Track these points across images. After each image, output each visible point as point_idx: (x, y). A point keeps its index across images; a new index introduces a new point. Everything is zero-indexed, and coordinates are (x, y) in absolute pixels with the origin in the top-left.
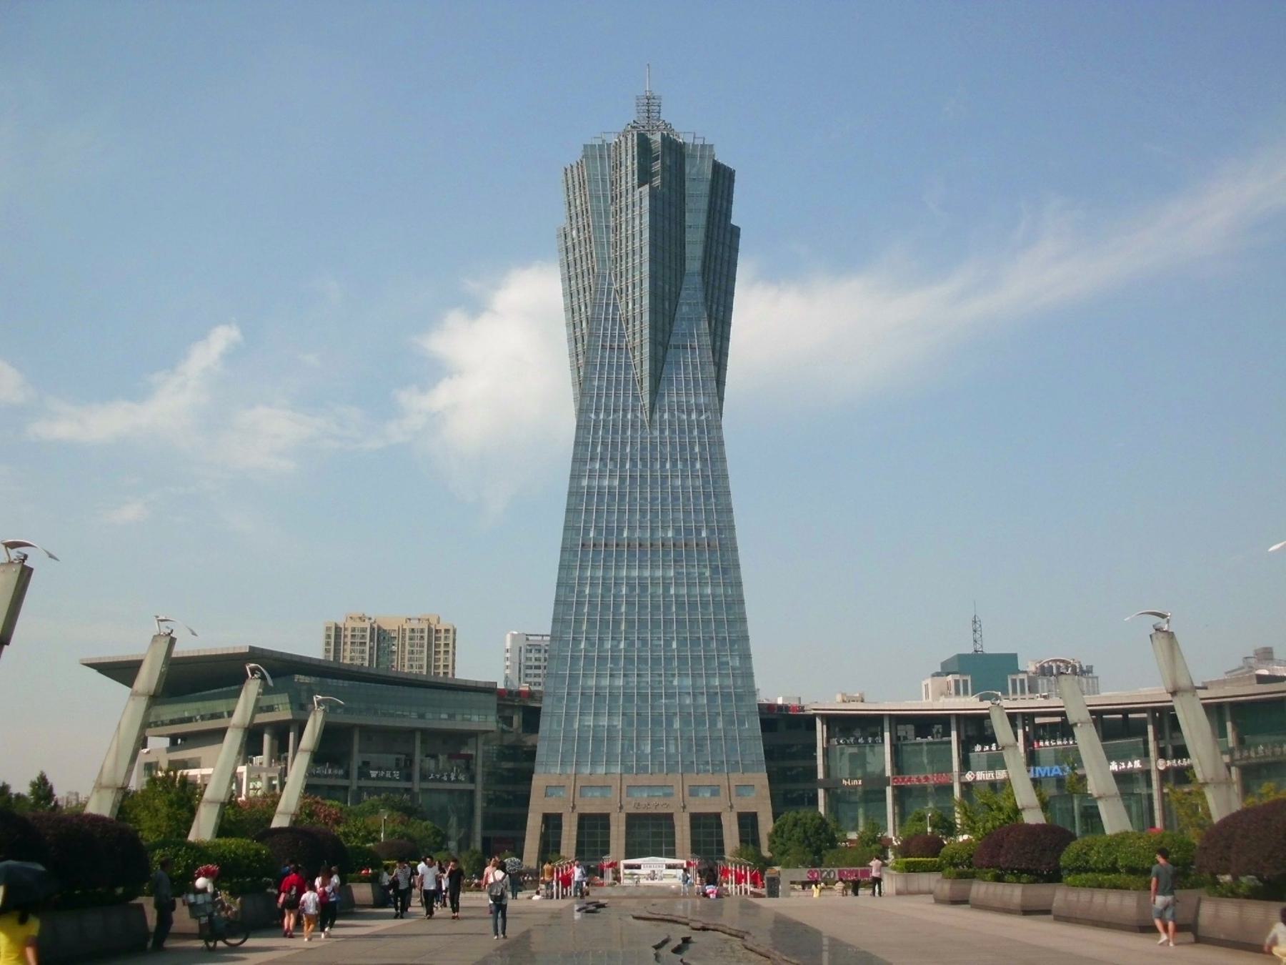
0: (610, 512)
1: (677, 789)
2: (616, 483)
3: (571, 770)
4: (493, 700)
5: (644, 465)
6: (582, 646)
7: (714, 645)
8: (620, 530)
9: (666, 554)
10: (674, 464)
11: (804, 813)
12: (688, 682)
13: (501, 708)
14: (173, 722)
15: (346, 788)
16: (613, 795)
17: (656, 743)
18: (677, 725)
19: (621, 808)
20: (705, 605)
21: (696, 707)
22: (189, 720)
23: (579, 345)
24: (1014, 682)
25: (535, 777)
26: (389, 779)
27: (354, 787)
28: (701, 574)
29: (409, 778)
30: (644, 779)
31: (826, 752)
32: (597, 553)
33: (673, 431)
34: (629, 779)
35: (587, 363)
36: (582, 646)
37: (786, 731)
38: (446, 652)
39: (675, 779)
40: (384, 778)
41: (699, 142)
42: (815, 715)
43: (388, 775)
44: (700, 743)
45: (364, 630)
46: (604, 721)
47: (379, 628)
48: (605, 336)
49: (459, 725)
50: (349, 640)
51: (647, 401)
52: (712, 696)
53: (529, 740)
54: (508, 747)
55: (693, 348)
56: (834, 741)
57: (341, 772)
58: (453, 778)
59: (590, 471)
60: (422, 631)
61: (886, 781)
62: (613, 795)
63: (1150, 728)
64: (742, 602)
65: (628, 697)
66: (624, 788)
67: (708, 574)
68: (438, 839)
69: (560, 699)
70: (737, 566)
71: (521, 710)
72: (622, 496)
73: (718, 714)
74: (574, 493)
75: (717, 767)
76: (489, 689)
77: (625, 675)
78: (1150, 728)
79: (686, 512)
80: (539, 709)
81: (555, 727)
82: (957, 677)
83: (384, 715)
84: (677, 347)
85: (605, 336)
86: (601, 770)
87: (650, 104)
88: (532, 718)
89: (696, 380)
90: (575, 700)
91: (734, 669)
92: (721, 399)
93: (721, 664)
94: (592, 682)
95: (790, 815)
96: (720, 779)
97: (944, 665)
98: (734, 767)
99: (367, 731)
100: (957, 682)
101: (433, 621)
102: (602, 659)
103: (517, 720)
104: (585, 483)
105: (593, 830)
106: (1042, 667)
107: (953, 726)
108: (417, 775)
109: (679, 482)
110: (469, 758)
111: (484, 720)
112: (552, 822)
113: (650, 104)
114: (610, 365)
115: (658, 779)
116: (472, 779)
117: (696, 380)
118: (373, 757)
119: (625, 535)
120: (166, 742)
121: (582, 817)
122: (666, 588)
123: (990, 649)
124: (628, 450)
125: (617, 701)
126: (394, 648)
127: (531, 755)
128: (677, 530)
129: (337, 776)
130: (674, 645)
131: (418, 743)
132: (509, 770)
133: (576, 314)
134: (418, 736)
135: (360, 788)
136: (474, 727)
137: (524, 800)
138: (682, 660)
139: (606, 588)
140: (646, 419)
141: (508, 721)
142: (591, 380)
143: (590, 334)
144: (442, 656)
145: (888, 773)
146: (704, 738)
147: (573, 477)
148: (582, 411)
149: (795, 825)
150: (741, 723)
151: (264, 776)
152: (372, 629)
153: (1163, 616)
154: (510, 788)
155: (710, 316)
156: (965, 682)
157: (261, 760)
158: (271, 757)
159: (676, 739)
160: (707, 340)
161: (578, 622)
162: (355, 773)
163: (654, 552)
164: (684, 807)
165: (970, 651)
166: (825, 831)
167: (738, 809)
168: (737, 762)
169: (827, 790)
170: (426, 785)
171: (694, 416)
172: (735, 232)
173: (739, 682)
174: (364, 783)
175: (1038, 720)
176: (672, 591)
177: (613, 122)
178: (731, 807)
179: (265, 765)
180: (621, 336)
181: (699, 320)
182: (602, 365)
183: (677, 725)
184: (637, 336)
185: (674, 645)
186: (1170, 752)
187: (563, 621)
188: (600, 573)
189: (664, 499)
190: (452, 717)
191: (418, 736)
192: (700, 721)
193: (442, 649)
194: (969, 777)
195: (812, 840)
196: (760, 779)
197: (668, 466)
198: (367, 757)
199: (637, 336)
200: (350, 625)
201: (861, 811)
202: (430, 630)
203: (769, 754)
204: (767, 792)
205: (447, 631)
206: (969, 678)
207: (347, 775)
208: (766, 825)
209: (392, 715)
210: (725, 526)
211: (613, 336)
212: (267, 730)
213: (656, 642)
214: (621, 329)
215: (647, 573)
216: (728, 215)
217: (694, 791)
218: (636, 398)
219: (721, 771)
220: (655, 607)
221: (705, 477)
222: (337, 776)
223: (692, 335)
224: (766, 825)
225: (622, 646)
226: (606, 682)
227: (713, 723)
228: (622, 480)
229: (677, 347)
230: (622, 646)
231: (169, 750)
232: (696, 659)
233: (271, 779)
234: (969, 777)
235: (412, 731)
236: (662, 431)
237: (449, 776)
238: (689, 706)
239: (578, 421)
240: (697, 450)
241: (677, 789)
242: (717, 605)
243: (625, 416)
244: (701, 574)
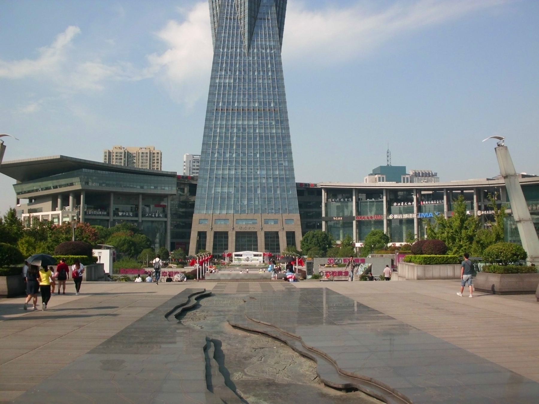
0: (229, 94)
1: (259, 221)
2: (232, 81)
3: (211, 212)
4: (175, 180)
5: (245, 73)
6: (216, 156)
7: (276, 156)
8: (234, 103)
9: (255, 114)
10: (259, 72)
11: (316, 231)
12: (264, 172)
13: (178, 184)
14: (29, 192)
15: (108, 220)
16: (230, 223)
17: (249, 200)
18: (259, 192)
19: (233, 229)
20: (272, 137)
21: (267, 184)
22: (37, 190)
23: (215, 18)
24: (404, 178)
25: (194, 215)
26: (128, 216)
27: (112, 220)
28: (271, 123)
29: (137, 215)
30: (244, 216)
31: (326, 205)
32: (223, 113)
33: (258, 58)
34: (237, 216)
35: (219, 26)
36: (216, 156)
37: (308, 196)
38: (158, 163)
39: (258, 216)
40: (125, 216)
42: (321, 188)
43: (127, 214)
44: (269, 200)
45: (121, 153)
46: (226, 190)
47: (128, 152)
48: (227, 13)
49: (159, 191)
50: (115, 157)
51: (246, 43)
52: (275, 179)
53: (192, 199)
54: (182, 202)
55: (268, 20)
56: (330, 200)
57: (105, 213)
58: (157, 216)
59: (220, 75)
60: (147, 153)
61: (353, 218)
62: (230, 223)
63: (475, 197)
64: (289, 136)
65: (237, 179)
66: (235, 220)
67: (274, 123)
68: (148, 243)
69: (206, 180)
70: (287, 120)
71: (188, 185)
72: (235, 87)
73: (278, 187)
74: (212, 85)
75: (277, 211)
76: (173, 175)
77: (235, 169)
78: (475, 197)
79: (264, 95)
80: (196, 185)
81: (203, 192)
82: (380, 176)
83: (125, 187)
84: (261, 19)
85: (227, 13)
86: (224, 212)
88: (193, 189)
89: (269, 34)
90: (212, 180)
91: (285, 167)
92: (281, 44)
93: (279, 164)
94: (220, 172)
95: (310, 233)
96: (278, 216)
97: (374, 170)
98: (285, 211)
99: (116, 194)
100: (379, 178)
101: (152, 149)
102: (225, 162)
103: (186, 189)
104: (217, 81)
105: (221, 238)
106: (416, 173)
107: (384, 194)
108: (140, 215)
109: (261, 81)
110: (164, 207)
111: (171, 189)
112: (202, 235)
114: (230, 27)
115: (250, 216)
116: (166, 216)
117: (269, 34)
118: (120, 207)
119: (236, 105)
120: (27, 201)
121: (216, 233)
122: (255, 130)
123: (393, 165)
124: (238, 66)
125: (232, 181)
126: (135, 161)
127: (193, 205)
128: (260, 103)
129: (104, 215)
130: (258, 156)
131: (141, 200)
132: (183, 212)
133: (214, 4)
134: (141, 197)
135: (114, 220)
136: (167, 193)
137: (190, 226)
138: (262, 162)
139: (227, 129)
140: (246, 52)
141: (183, 190)
142: (221, 33)
143: (220, 12)
144: (156, 164)
145: (354, 215)
146: (271, 198)
147: (212, 78)
148: (216, 48)
149: (313, 237)
150: (288, 191)
151: (70, 215)
152: (125, 153)
153: (500, 138)
154: (183, 220)
155: (276, 6)
156: (383, 178)
157: (69, 208)
158: (73, 206)
159: (259, 198)
160: (275, 16)
161: (214, 144)
162: (112, 214)
163: (249, 113)
164: (262, 229)
165: (386, 165)
166: (327, 240)
167: (287, 229)
169: (326, 222)
170: (144, 219)
171: (268, 51)
173: (287, 173)
174: (116, 218)
175: (423, 193)
176: (257, 131)
178: (283, 229)
179: (70, 210)
180: (235, 13)
181: (271, 6)
182: (226, 27)
183: (259, 192)
184: (242, 13)
185: (258, 156)
186: (483, 207)
187: (207, 144)
188: (224, 123)
189: (254, 89)
190: (156, 188)
191: (141, 197)
192: (269, 190)
193: (156, 161)
194: (391, 217)
195: (321, 244)
196: (296, 216)
197: (256, 74)
198: (117, 206)
199: (242, 13)
200: (115, 151)
201: (341, 231)
202: (150, 153)
203: (300, 206)
204: (299, 223)
205: (158, 153)
206: (385, 176)
207: (108, 214)
208: (299, 238)
209: (128, 187)
210: (283, 102)
211: (231, 13)
212: (71, 195)
213: (250, 154)
214: (235, 10)
215: (246, 123)
217: (266, 222)
218: (241, 42)
219: (279, 212)
220: (250, 138)
221: (273, 79)
222: (104, 215)
223: (268, 13)
224: (299, 238)
225: (234, 156)
226: (227, 172)
227: (275, 191)
228: (235, 80)
229: (261, 19)
230: (234, 156)
231: (29, 205)
232: (268, 162)
233: (73, 217)
234: (391, 217)
235: (138, 195)
236: (253, 58)
237: (155, 215)
238: (264, 183)
239: (215, 53)
240: (269, 66)
241: (259, 221)
242: (278, 138)
243: (236, 50)
244: (271, 123)
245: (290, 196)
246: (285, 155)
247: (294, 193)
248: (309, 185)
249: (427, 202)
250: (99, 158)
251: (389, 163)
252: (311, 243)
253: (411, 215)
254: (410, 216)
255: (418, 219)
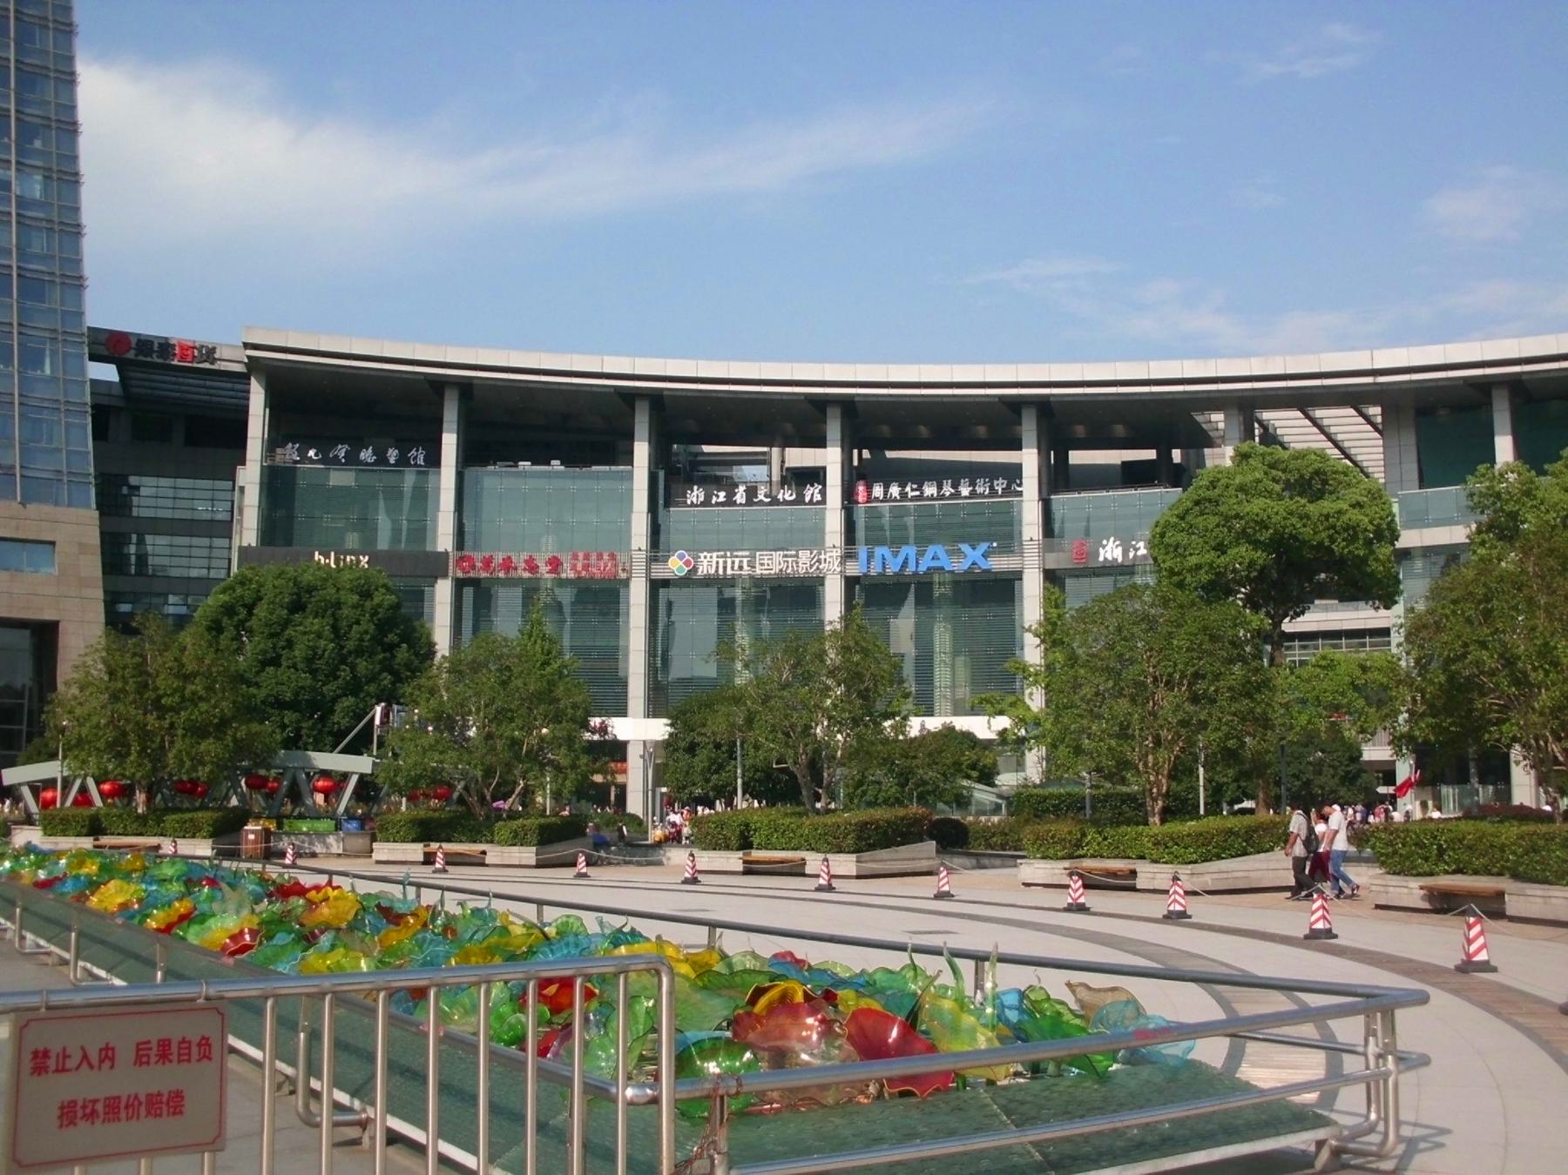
37: (164, 410)
61: (436, 566)
91: (22, 202)
145: (444, 540)
149: (297, 606)
150: (31, 359)
168: (9, 472)
173: (38, 244)
234: (675, 566)
245: (41, 392)
246: (27, 132)
248: (165, 347)
249: (895, 490)
252: (275, 662)
253: (804, 556)
254: (802, 563)
255: (850, 583)
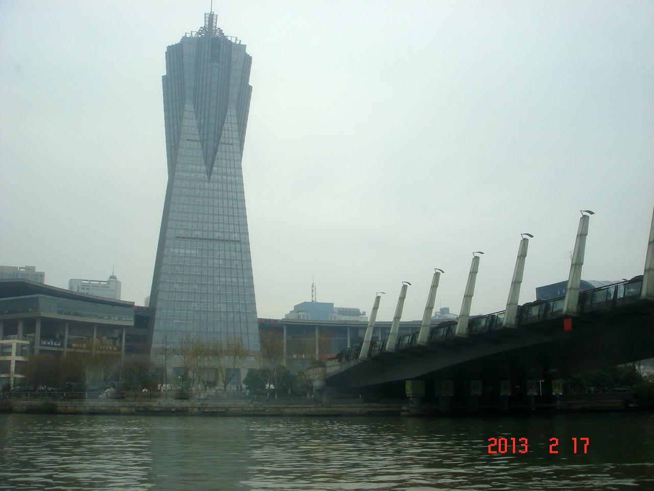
41: (238, 43)
71: (144, 318)
76: (130, 305)
87: (211, 18)
113: (211, 18)
123: (318, 301)
165: (310, 301)
172: (250, 89)
177: (193, 26)
207: (62, 346)
216: (248, 80)
222: (57, 346)
235: (93, 324)
247: (255, 329)
250: (64, 285)
251: (314, 299)
